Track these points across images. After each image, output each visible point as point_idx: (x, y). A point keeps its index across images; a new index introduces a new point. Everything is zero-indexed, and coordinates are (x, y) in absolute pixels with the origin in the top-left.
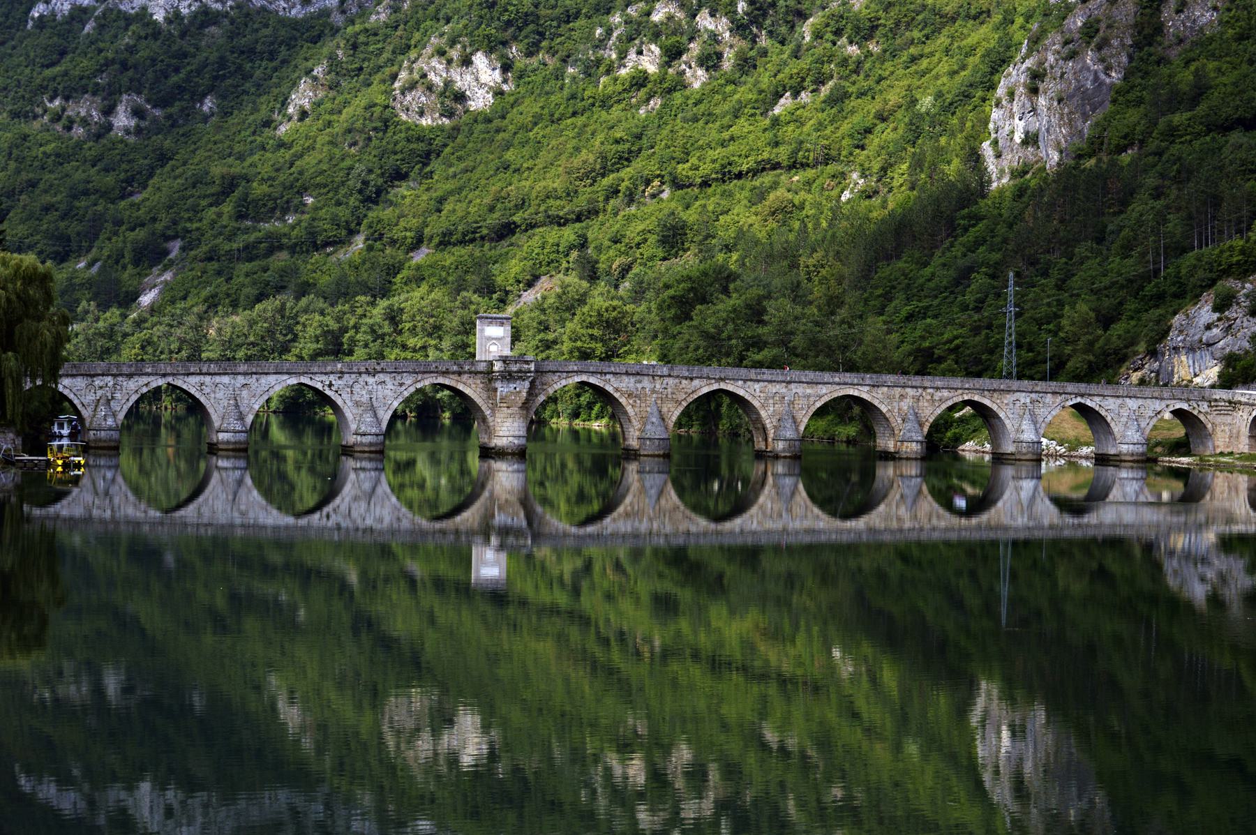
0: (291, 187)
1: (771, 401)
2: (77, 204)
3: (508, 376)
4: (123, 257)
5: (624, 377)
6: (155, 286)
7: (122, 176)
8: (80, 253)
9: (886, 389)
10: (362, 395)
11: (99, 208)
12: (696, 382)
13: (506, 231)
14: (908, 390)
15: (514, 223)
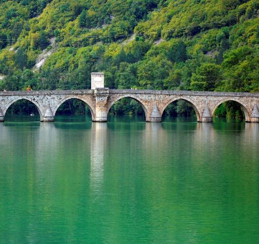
0: (105, 12)
1: (200, 103)
2: (10, 21)
3: (99, 95)
4: (30, 45)
5: (144, 95)
6: (43, 58)
7: (31, 7)
8: (12, 43)
9: (245, 98)
10: (46, 103)
11: (21, 22)
12: (171, 96)
13: (195, 31)
14: (254, 98)
15: (200, 27)
